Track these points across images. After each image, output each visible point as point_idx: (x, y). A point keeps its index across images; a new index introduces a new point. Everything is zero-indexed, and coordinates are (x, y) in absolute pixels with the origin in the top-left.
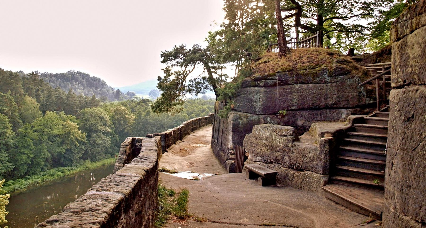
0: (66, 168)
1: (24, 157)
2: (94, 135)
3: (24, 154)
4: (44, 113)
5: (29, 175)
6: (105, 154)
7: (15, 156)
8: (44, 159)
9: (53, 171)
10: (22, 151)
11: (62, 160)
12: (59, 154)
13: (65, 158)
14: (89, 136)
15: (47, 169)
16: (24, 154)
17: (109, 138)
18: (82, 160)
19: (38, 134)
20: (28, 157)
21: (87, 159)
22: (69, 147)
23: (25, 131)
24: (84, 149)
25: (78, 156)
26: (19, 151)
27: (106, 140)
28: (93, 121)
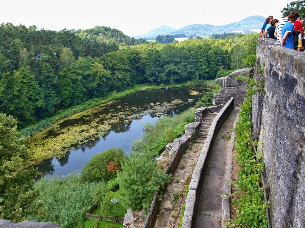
0: (99, 99)
1: (67, 92)
2: (116, 72)
3: (67, 90)
4: (77, 58)
5: (74, 105)
6: (127, 86)
8: (82, 92)
9: (90, 101)
10: (64, 88)
11: (95, 93)
12: (93, 89)
13: (97, 91)
14: (113, 74)
16: (67, 90)
17: (128, 74)
18: (110, 92)
19: (74, 74)
20: (71, 93)
21: (114, 91)
22: (98, 82)
23: (64, 74)
24: (111, 83)
25: (107, 89)
26: (62, 88)
27: (126, 75)
28: (115, 62)
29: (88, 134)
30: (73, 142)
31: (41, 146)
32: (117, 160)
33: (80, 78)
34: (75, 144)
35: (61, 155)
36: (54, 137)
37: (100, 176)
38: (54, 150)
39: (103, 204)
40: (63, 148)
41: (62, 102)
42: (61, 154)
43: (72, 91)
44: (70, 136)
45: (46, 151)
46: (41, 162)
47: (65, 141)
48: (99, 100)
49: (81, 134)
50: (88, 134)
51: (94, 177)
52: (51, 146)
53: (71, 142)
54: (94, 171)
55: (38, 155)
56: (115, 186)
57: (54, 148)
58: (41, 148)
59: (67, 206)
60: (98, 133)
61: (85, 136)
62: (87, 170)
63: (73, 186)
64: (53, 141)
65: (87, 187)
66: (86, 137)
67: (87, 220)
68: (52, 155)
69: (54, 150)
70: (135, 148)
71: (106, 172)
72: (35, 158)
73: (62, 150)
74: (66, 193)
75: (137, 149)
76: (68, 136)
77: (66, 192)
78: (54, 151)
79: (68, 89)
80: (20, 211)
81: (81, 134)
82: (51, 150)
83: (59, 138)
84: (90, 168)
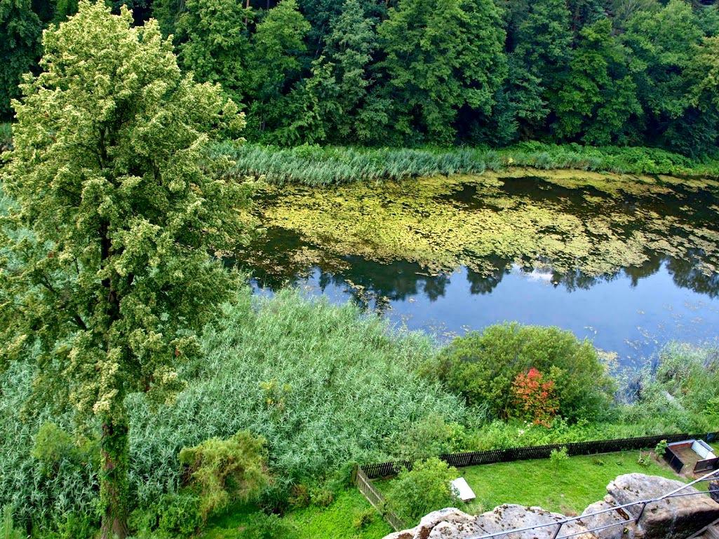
0: (671, 155)
3: (581, 90)
5: (583, 144)
7: (561, 89)
9: (637, 151)
10: (576, 81)
11: (670, 132)
12: (665, 115)
13: (679, 128)
15: (625, 142)
16: (581, 90)
20: (589, 101)
22: (694, 102)
23: (594, 35)
26: (571, 78)
29: (560, 246)
30: (502, 248)
31: (415, 216)
32: (559, 375)
33: (640, 66)
34: (503, 257)
35: (445, 266)
36: (465, 209)
37: (483, 393)
38: (438, 244)
39: (406, 477)
40: (465, 250)
41: (553, 117)
42: (446, 264)
43: (595, 99)
44: (507, 228)
45: (419, 236)
46: (382, 259)
47: (485, 235)
48: (669, 158)
49: (540, 238)
50: (560, 246)
51: (466, 383)
52: (438, 229)
53: (498, 244)
54: (474, 367)
55: (393, 235)
56: (498, 448)
57: (443, 239)
58: (413, 222)
59: (340, 415)
60: (591, 258)
61: (547, 248)
62: (461, 351)
63: (396, 371)
64: (453, 218)
65: (428, 397)
66: (547, 251)
67: (353, 490)
68: (423, 255)
69: (438, 244)
70: (662, 369)
71: (505, 391)
72: (377, 240)
73: (458, 256)
74: (367, 381)
75: (668, 377)
76: (502, 226)
77: (367, 381)
78: (437, 247)
79: (586, 85)
80: (110, 372)
81: (542, 235)
82: (431, 241)
83: (475, 217)
84: (469, 351)
